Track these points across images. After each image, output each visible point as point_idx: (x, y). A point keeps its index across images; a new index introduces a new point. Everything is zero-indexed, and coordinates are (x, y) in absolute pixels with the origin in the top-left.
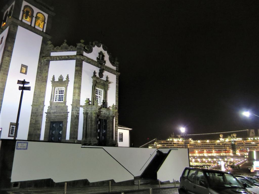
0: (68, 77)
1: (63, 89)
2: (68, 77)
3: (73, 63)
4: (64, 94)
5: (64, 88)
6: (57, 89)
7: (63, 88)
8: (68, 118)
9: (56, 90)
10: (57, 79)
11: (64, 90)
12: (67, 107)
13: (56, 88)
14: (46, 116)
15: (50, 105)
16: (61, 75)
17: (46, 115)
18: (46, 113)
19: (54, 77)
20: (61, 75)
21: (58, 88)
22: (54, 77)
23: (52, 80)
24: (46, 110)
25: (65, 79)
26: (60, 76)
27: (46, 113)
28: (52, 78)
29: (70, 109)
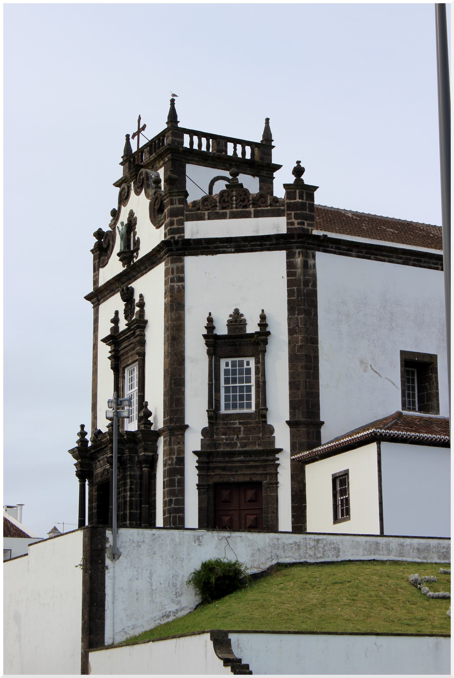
0: (263, 317)
1: (248, 364)
2: (263, 317)
4: (253, 382)
6: (227, 365)
8: (279, 470)
9: (223, 366)
10: (222, 329)
11: (252, 365)
13: (223, 362)
14: (197, 465)
15: (207, 425)
16: (237, 311)
17: (198, 462)
18: (195, 453)
19: (210, 320)
22: (210, 320)
23: (205, 332)
24: (193, 441)
25: (252, 327)
26: (231, 316)
27: (195, 453)
28: (206, 323)
29: (282, 438)
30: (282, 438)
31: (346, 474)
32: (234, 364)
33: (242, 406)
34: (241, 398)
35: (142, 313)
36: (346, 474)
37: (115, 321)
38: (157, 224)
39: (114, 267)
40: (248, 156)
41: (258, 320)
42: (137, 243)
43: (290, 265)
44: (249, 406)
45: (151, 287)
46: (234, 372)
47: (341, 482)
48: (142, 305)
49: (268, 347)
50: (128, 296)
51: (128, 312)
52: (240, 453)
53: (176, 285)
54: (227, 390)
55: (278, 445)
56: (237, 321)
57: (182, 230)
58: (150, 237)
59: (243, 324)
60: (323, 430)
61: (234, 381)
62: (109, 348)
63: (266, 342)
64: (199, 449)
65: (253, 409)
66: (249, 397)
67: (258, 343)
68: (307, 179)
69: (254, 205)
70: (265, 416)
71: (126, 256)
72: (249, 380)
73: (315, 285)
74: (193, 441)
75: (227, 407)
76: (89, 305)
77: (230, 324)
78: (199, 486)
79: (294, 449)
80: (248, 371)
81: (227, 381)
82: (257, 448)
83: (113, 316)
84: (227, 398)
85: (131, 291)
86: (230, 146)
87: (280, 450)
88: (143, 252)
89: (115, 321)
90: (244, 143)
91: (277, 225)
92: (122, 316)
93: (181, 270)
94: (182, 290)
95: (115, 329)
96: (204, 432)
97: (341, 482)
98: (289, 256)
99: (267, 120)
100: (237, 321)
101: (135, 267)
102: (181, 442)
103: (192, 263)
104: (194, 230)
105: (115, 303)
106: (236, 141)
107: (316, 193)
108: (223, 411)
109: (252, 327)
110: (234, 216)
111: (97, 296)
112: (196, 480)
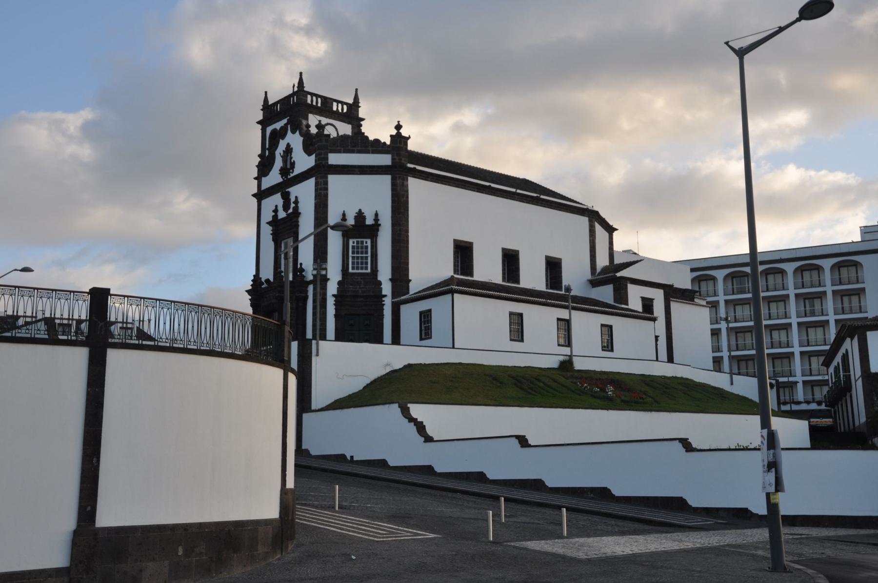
0: (376, 215)
2: (376, 215)
3: (384, 182)
5: (369, 241)
7: (365, 240)
8: (385, 307)
9: (351, 244)
10: (351, 221)
11: (369, 244)
12: (380, 283)
13: (351, 241)
16: (360, 210)
19: (344, 215)
20: (360, 210)
21: (355, 240)
24: (332, 288)
25: (369, 221)
27: (334, 295)
29: (387, 288)
30: (387, 288)
31: (430, 311)
32: (358, 242)
33: (362, 269)
34: (362, 263)
35: (296, 209)
36: (430, 311)
37: (276, 211)
38: (309, 154)
39: (274, 178)
40: (345, 110)
41: (373, 217)
42: (293, 165)
43: (394, 185)
44: (366, 268)
45: (304, 193)
46: (358, 248)
47: (426, 317)
48: (296, 202)
49: (379, 233)
50: (286, 197)
51: (286, 207)
52: (361, 297)
53: (323, 192)
54: (353, 258)
55: (384, 293)
56: (360, 216)
57: (327, 159)
58: (303, 162)
59: (364, 218)
60: (411, 284)
61: (358, 253)
62: (271, 228)
63: (378, 230)
64: (335, 293)
65: (369, 271)
66: (367, 263)
67: (372, 231)
68: (404, 132)
69: (372, 146)
70: (376, 275)
71: (284, 171)
72: (367, 253)
73: (407, 197)
74: (332, 288)
75: (353, 268)
76: (255, 200)
77: (356, 218)
78: (336, 316)
79: (394, 294)
80: (367, 247)
81: (353, 253)
82: (371, 294)
83: (274, 208)
84: (353, 263)
85: (288, 193)
86: (335, 104)
87: (385, 296)
88: (298, 170)
89: (276, 211)
90: (343, 103)
91: (385, 160)
92: (280, 208)
93: (326, 183)
94: (326, 196)
95: (275, 217)
96: (339, 283)
97: (426, 317)
98: (393, 179)
99: (356, 90)
100: (360, 216)
101: (290, 180)
102: (324, 288)
103: (333, 180)
104: (335, 159)
105: (277, 199)
106: (338, 102)
107: (409, 142)
108: (350, 270)
109: (369, 221)
110: (359, 152)
111: (261, 195)
112: (334, 312)
